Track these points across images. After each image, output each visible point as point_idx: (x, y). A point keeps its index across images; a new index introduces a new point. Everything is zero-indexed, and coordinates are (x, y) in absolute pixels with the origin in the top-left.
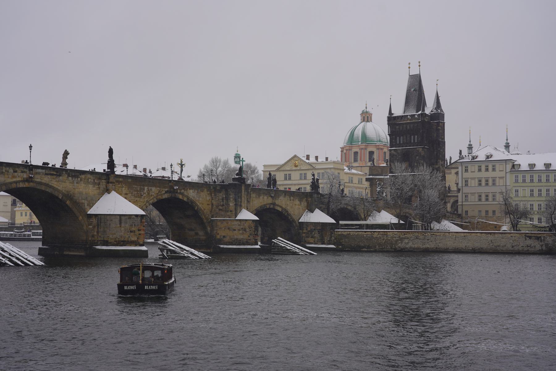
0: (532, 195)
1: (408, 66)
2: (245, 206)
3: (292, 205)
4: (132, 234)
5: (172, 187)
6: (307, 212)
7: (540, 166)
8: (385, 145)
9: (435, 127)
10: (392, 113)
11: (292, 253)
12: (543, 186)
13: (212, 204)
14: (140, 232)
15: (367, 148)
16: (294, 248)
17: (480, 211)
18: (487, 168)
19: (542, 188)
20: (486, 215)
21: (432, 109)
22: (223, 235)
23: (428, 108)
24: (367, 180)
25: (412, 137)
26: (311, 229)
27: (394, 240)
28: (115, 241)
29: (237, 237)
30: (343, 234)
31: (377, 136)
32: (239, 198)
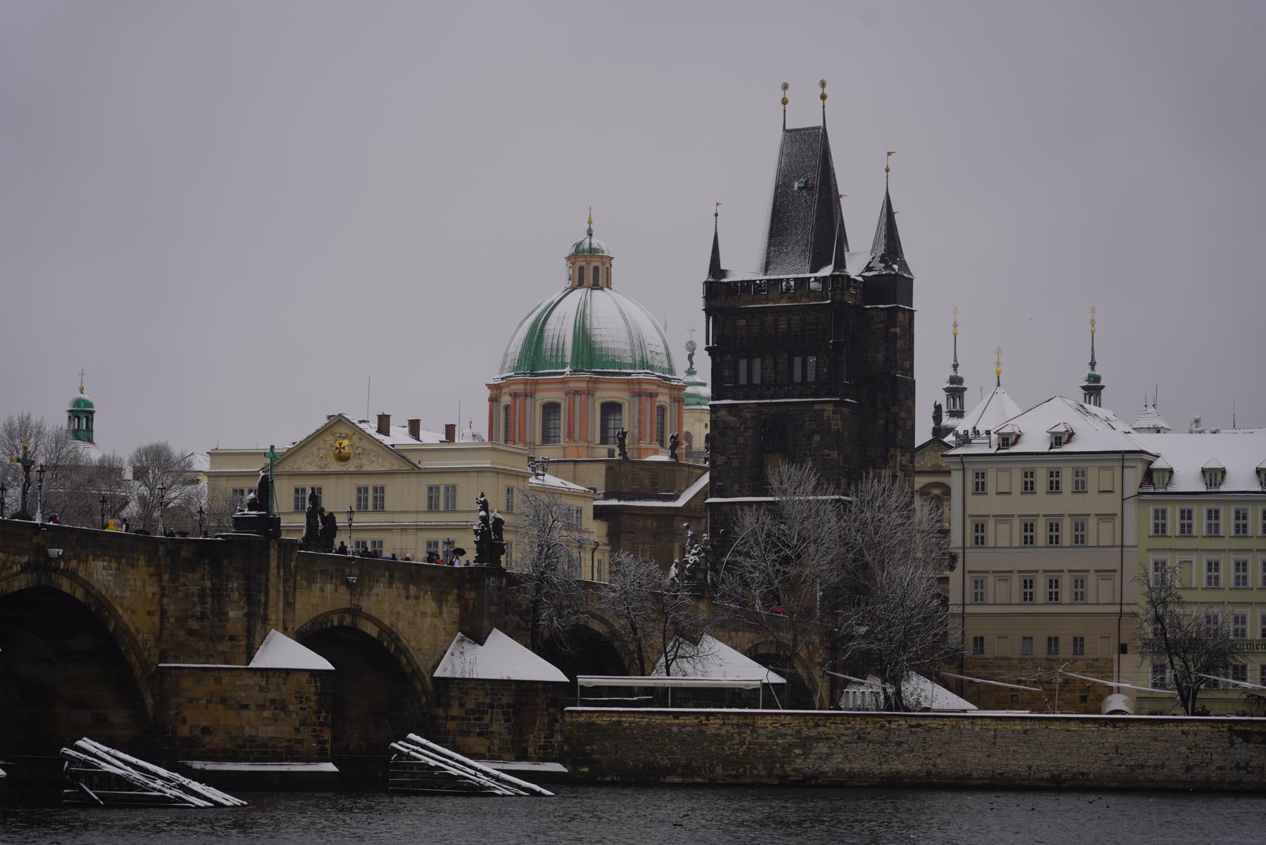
0: (1213, 582)
2: (277, 620)
3: (411, 614)
5: (41, 550)
6: (462, 640)
8: (665, 378)
9: (882, 326)
10: (722, 268)
12: (1252, 550)
13: (163, 613)
15: (595, 390)
16: (473, 772)
17: (1028, 640)
18: (1055, 479)
19: (1249, 557)
20: (1049, 652)
21: (869, 259)
22: (204, 723)
23: (853, 254)
24: (599, 513)
25: (798, 361)
27: (778, 745)
29: (254, 733)
30: (594, 722)
31: (632, 344)
32: (259, 591)
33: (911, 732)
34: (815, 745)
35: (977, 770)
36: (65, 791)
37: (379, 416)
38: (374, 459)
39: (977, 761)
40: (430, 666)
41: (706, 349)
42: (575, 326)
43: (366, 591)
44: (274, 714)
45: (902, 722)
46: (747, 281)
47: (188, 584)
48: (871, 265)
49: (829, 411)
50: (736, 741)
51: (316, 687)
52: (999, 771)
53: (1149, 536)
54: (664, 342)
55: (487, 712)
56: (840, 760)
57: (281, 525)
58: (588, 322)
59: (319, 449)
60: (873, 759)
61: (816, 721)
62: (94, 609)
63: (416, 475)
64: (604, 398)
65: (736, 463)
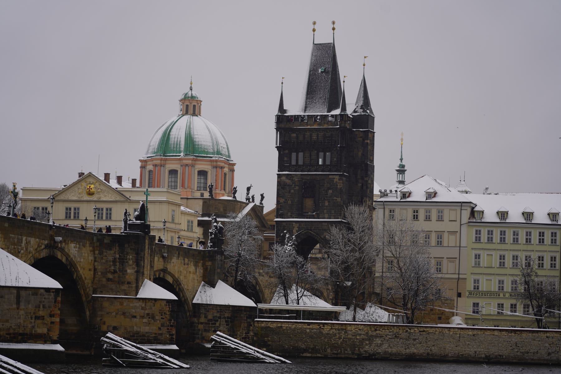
0: (502, 265)
1: (312, 27)
2: (147, 275)
3: (185, 272)
4: (39, 321)
5: (52, 238)
6: (204, 285)
7: (515, 217)
9: (361, 139)
10: (285, 108)
11: (250, 359)
13: (95, 270)
14: (53, 319)
15: (195, 164)
21: (355, 107)
22: (114, 324)
24: (200, 223)
26: (214, 317)
27: (357, 339)
28: (7, 334)
29: (138, 330)
32: (141, 260)
33: (420, 334)
34: (375, 339)
35: (451, 352)
36: (103, 359)
37: (105, 174)
38: (107, 195)
39: (451, 348)
40: (191, 298)
41: (277, 147)
42: (186, 133)
43: (169, 261)
44: (148, 321)
45: (416, 329)
46: (298, 115)
47: (107, 256)
48: (356, 110)
49: (336, 179)
50: (337, 337)
51: (169, 308)
52: (462, 354)
53: (473, 242)
54: (226, 142)
55: (218, 321)
56: (386, 347)
57: (151, 227)
58: (192, 132)
59: (78, 189)
60: (402, 347)
61: (375, 328)
62: (69, 267)
63: (128, 203)
64: (199, 168)
65: (290, 202)
